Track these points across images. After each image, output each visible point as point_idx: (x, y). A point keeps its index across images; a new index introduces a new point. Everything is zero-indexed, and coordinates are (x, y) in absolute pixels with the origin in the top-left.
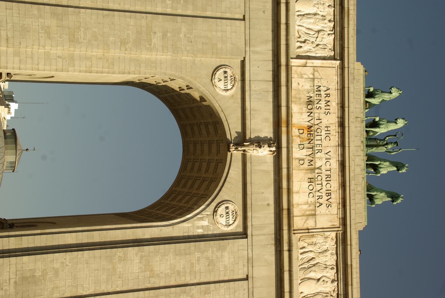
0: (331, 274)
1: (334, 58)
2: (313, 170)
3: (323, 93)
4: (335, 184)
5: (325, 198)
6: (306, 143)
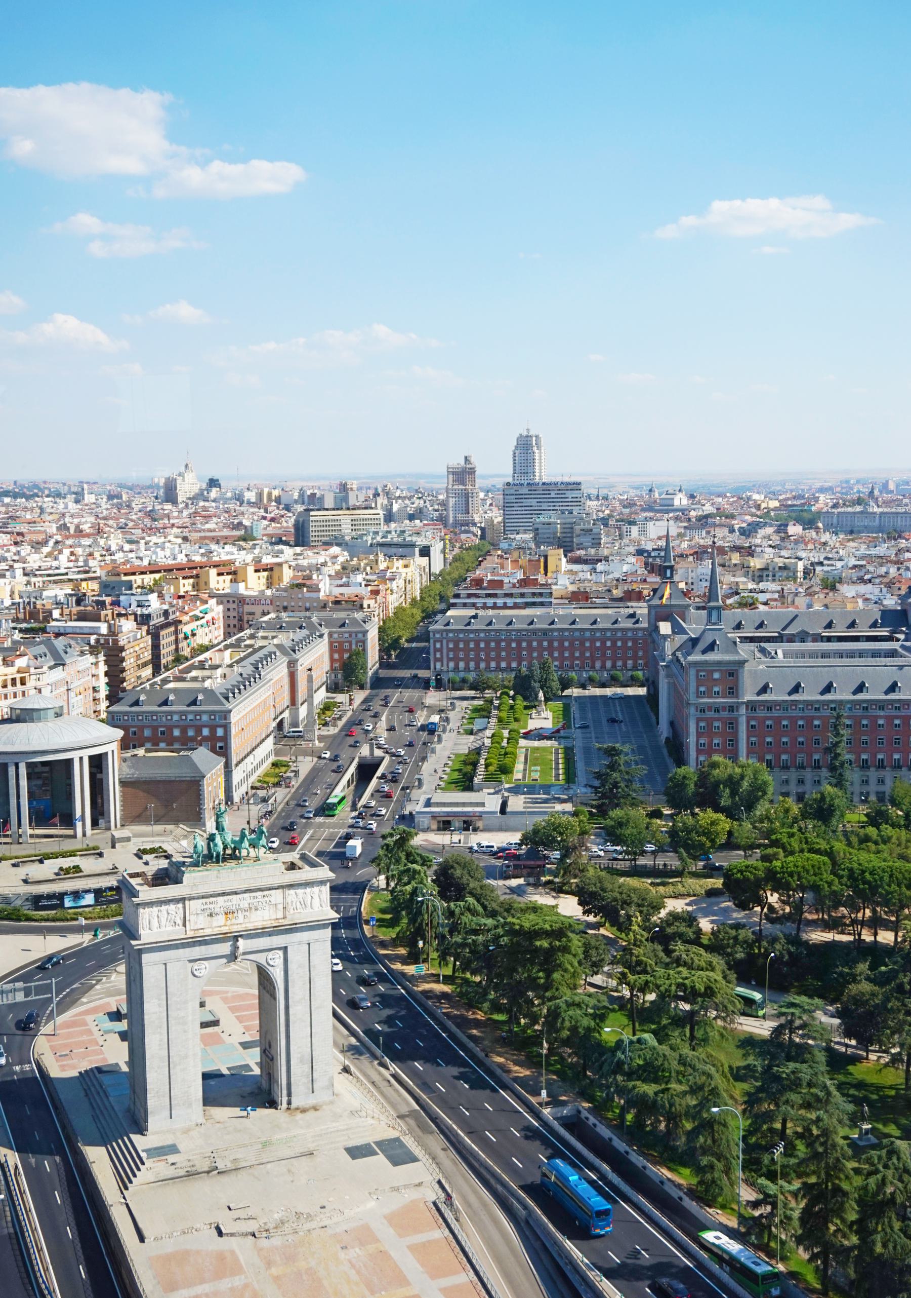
0: (308, 890)
1: (184, 904)
2: (250, 908)
3: (206, 907)
4: (259, 894)
5: (266, 899)
6: (235, 915)
